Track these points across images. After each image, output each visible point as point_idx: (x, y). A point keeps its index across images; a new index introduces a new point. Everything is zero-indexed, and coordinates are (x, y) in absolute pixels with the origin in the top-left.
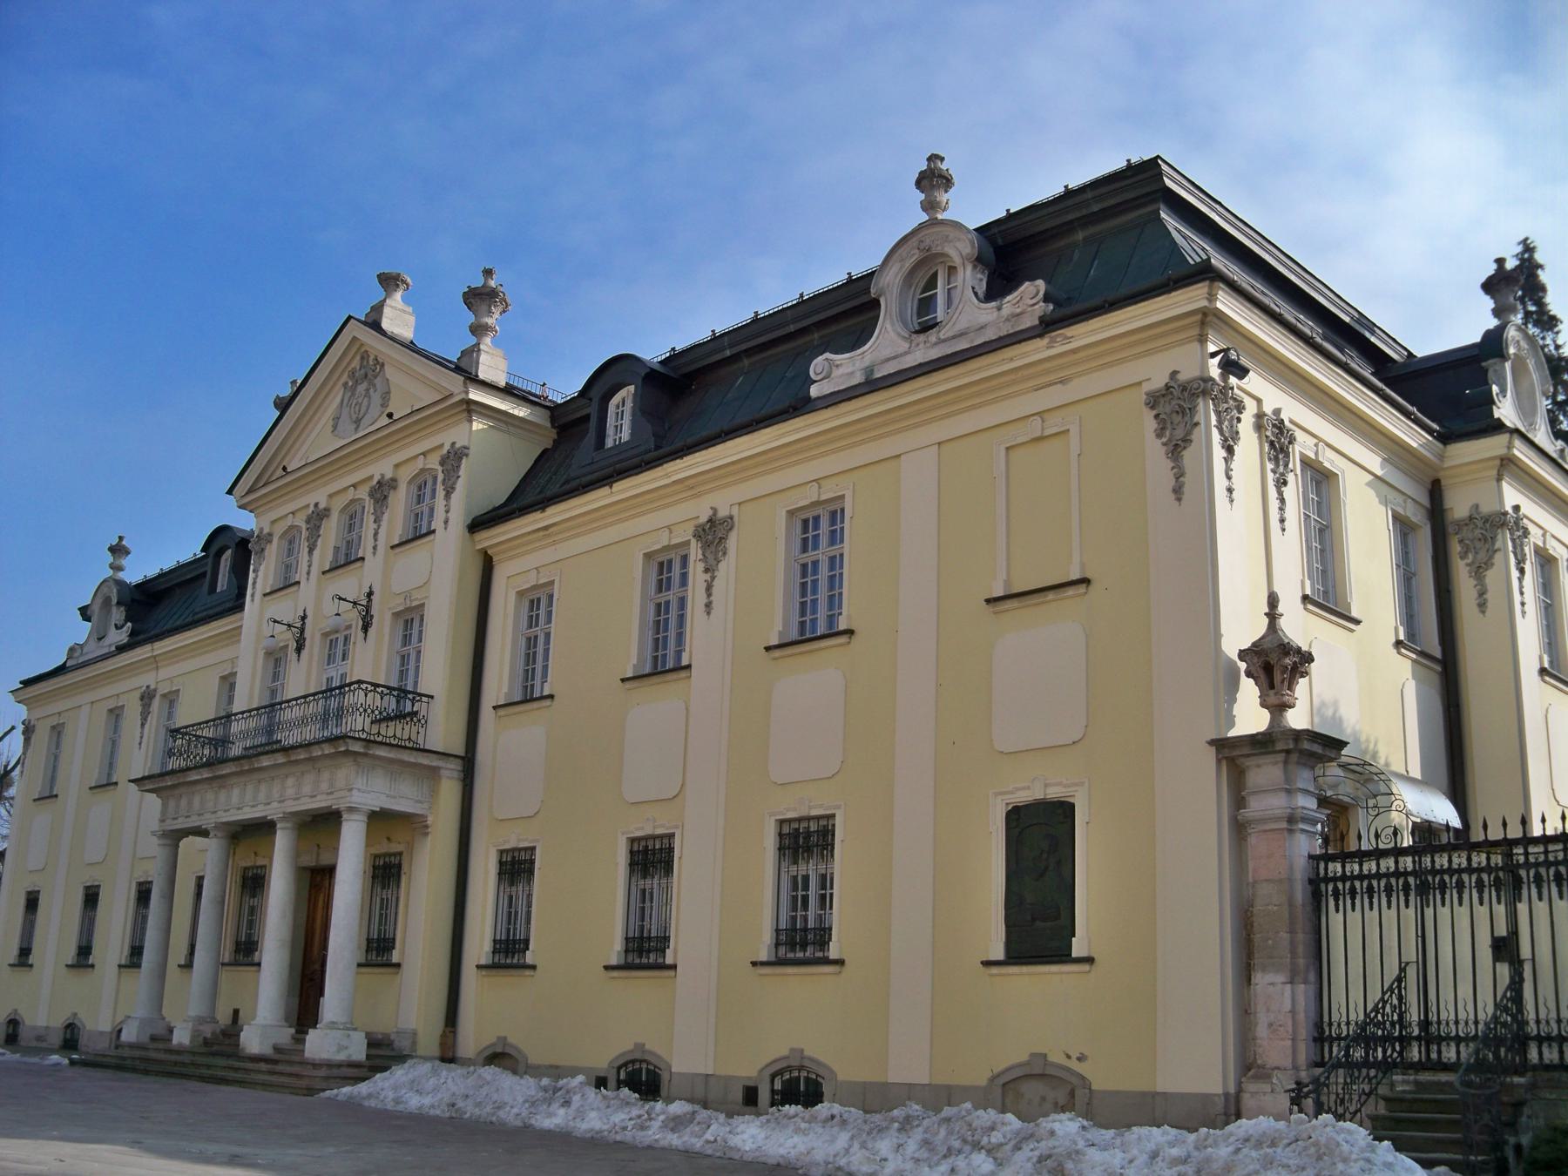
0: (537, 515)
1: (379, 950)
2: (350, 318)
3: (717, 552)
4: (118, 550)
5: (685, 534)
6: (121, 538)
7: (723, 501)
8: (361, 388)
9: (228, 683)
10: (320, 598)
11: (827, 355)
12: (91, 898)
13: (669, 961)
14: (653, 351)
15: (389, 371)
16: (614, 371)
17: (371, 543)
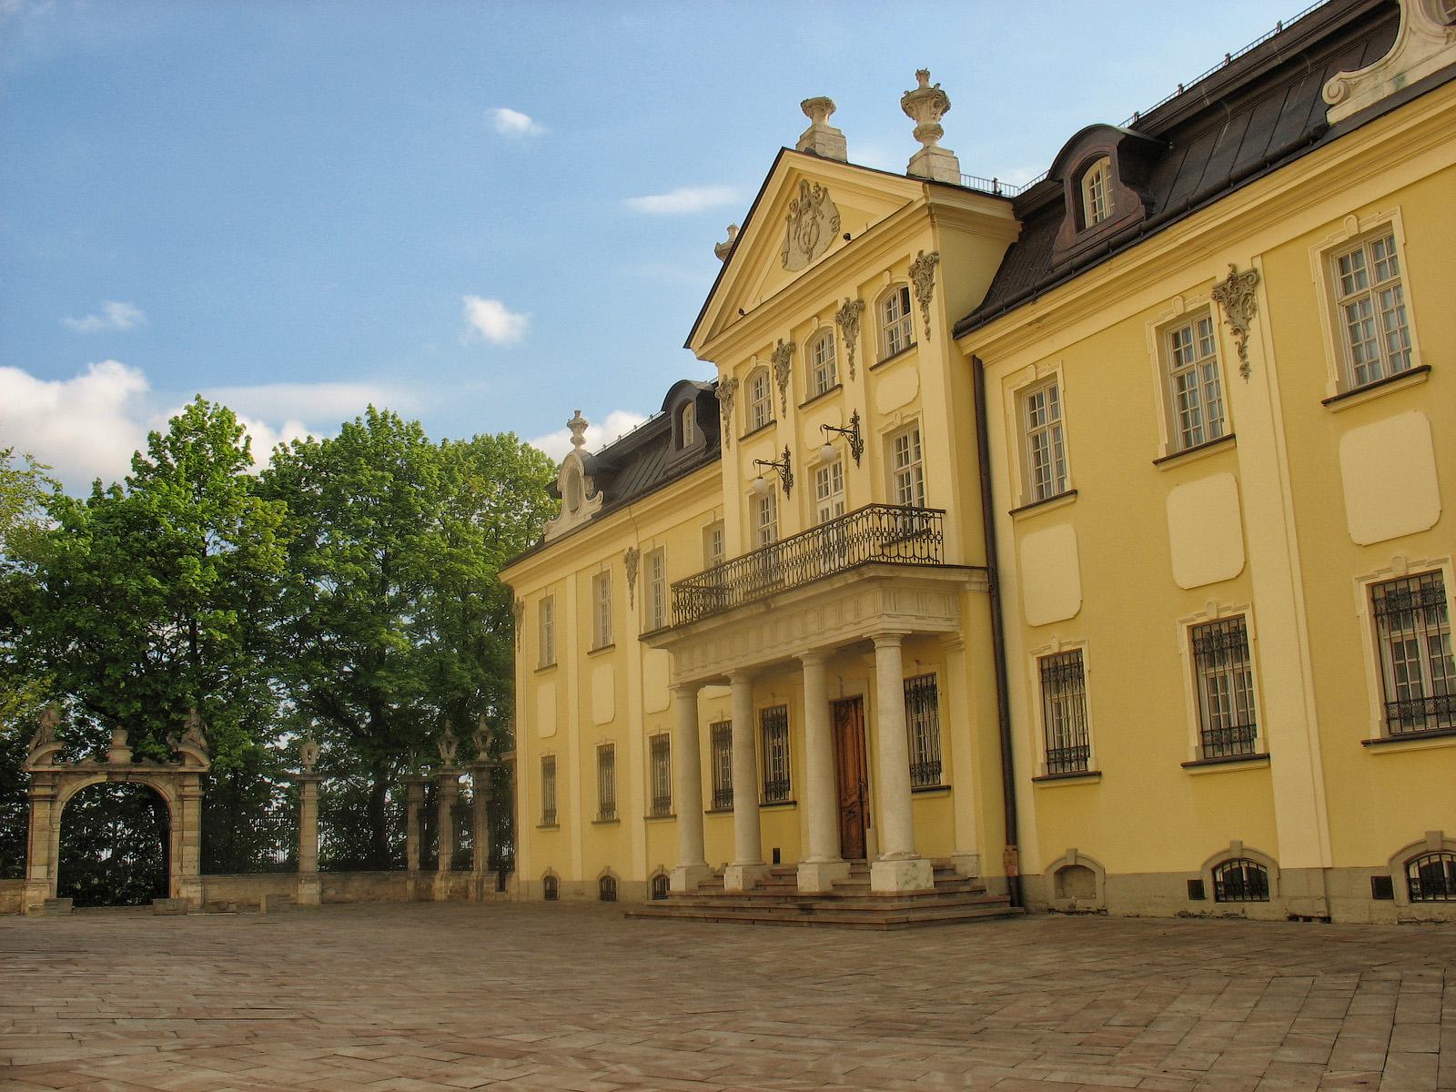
0: (1028, 309)
1: (926, 775)
2: (783, 149)
3: (1244, 310)
5: (1204, 297)
6: (578, 413)
7: (1243, 257)
8: (807, 218)
9: (714, 533)
10: (806, 434)
11: (1342, 74)
12: (606, 757)
13: (1259, 750)
14: (1120, 117)
15: (835, 196)
16: (1079, 150)
17: (846, 368)
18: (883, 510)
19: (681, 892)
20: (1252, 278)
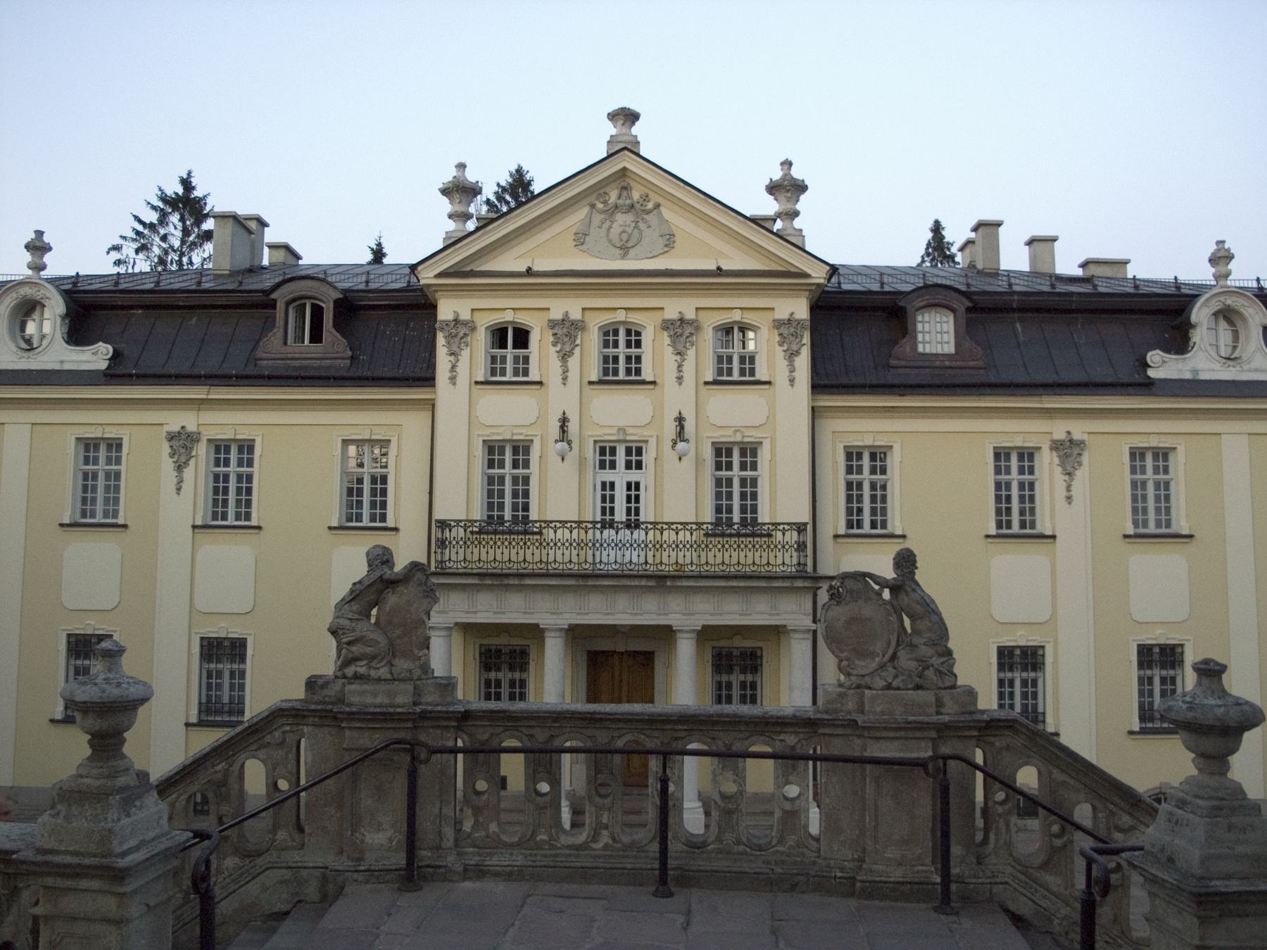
4: (38, 247)
11: (1158, 351)
20: (1080, 444)
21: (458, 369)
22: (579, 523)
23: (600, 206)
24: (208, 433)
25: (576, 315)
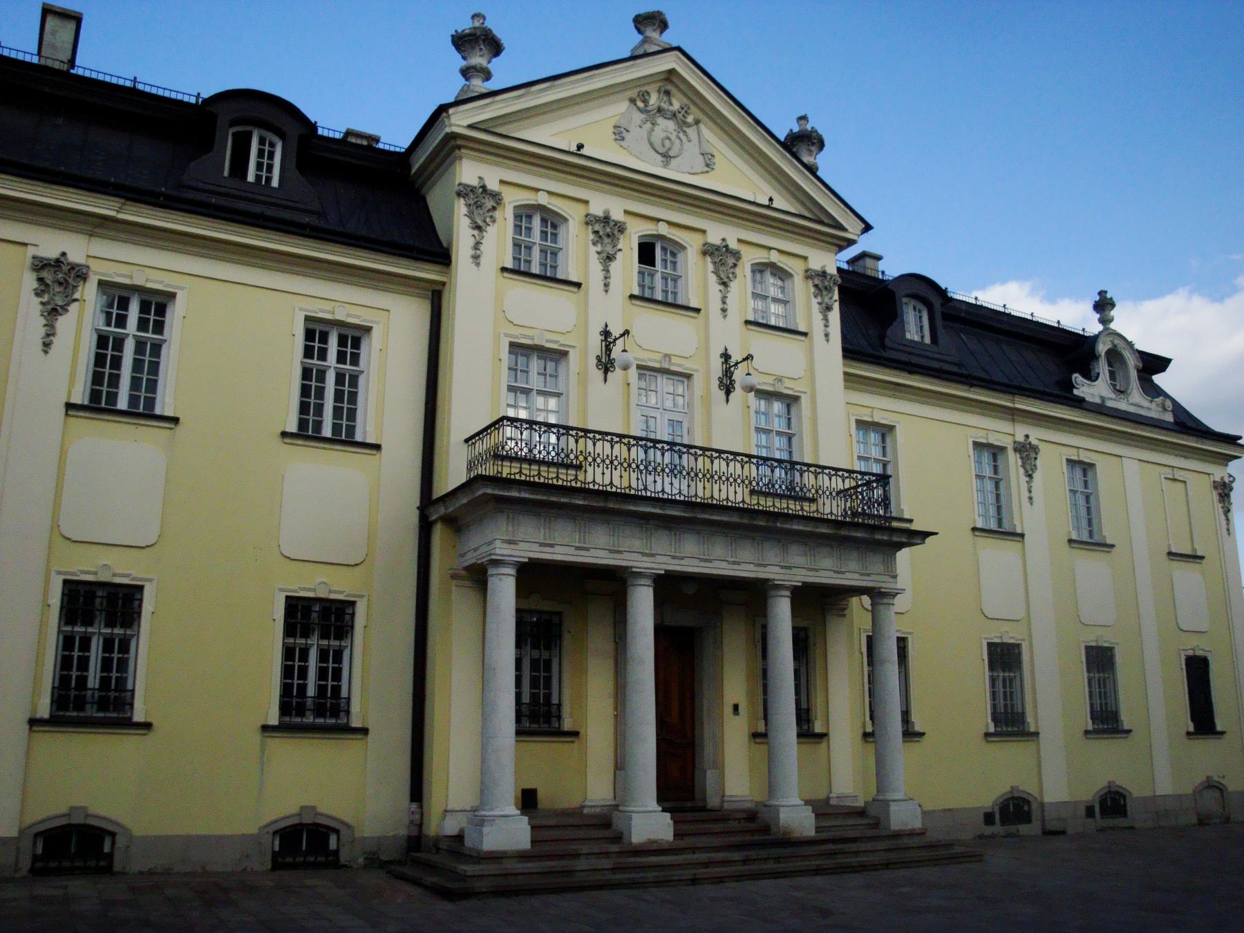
17: (715, 305)
18: (699, 452)
19: (524, 851)
20: (1035, 449)
21: (482, 247)
22: (672, 444)
23: (640, 104)
24: (99, 271)
25: (617, 215)
